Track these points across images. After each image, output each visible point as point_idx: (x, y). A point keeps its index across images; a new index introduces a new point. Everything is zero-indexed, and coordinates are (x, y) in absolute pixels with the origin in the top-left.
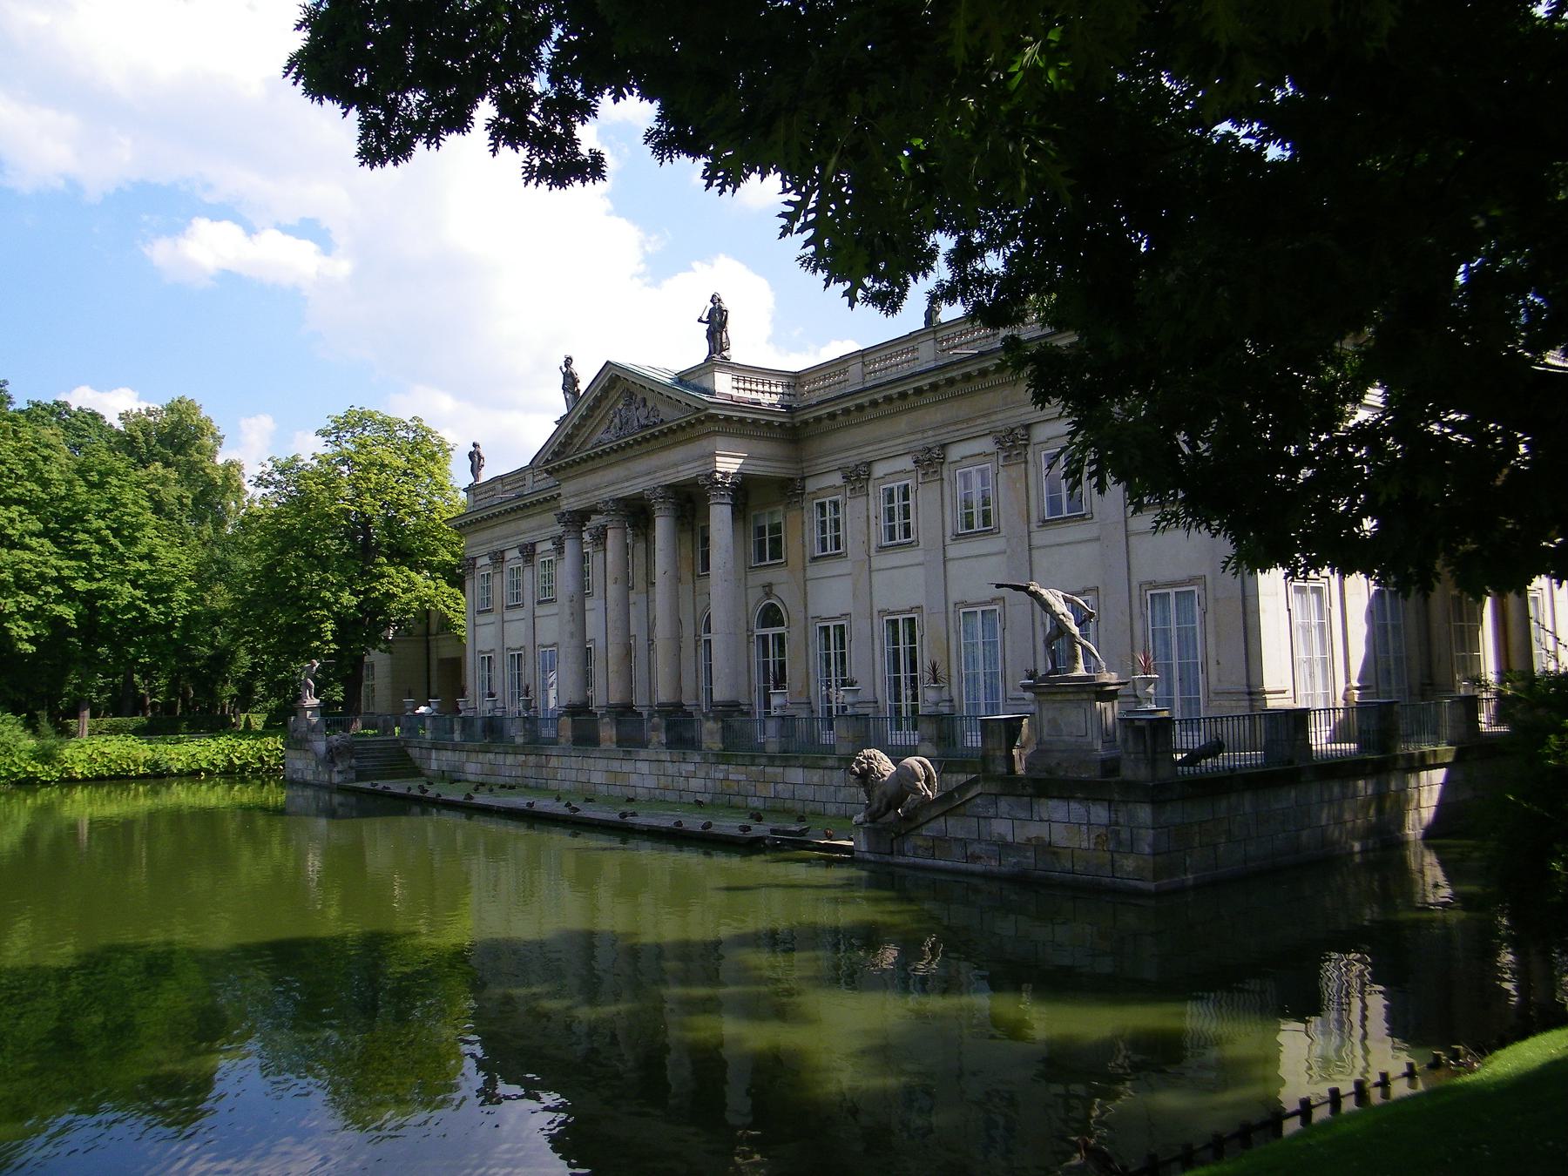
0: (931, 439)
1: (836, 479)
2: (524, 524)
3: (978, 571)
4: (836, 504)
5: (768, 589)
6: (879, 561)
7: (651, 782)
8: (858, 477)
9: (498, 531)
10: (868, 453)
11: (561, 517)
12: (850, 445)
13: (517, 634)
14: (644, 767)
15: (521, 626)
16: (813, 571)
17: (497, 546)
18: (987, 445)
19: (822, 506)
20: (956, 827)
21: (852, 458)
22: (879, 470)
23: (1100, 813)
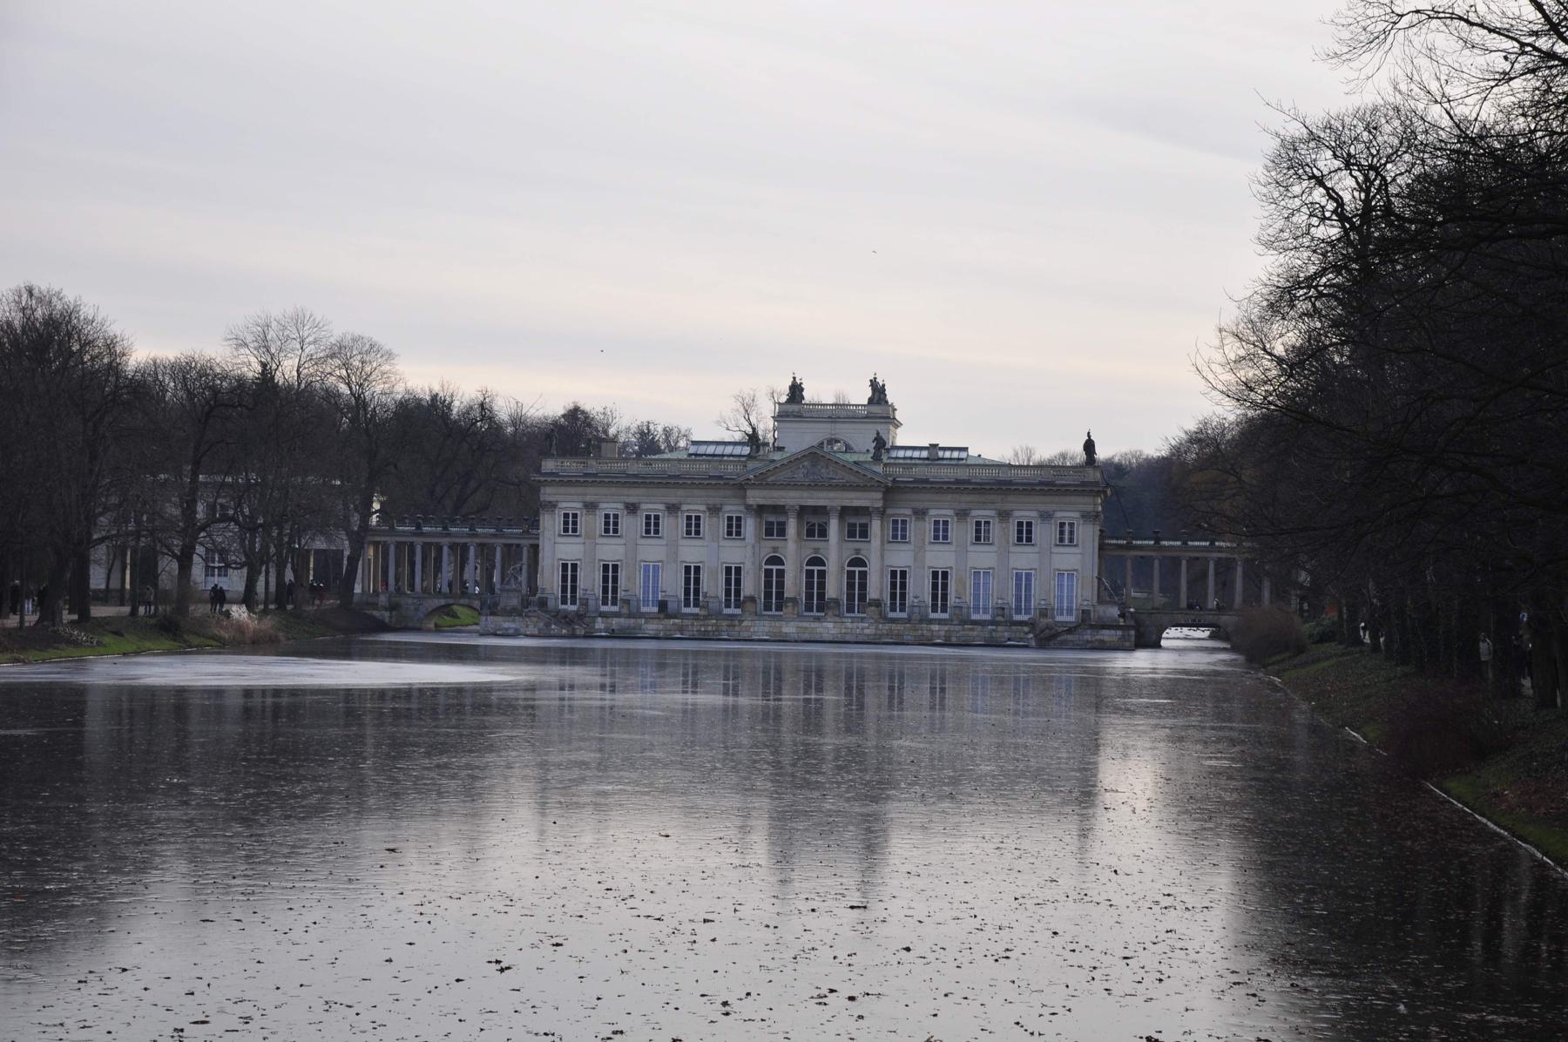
0: (964, 506)
1: (908, 512)
2: (625, 491)
3: (983, 557)
4: (904, 522)
5: (858, 551)
6: (929, 547)
7: (834, 631)
8: (920, 514)
9: (591, 490)
10: (927, 505)
11: (748, 507)
12: (921, 500)
13: (611, 550)
14: (831, 625)
15: (621, 550)
16: (888, 546)
17: (588, 499)
18: (992, 513)
19: (895, 522)
20: (1069, 637)
21: (919, 505)
22: (932, 512)
23: (1119, 633)
